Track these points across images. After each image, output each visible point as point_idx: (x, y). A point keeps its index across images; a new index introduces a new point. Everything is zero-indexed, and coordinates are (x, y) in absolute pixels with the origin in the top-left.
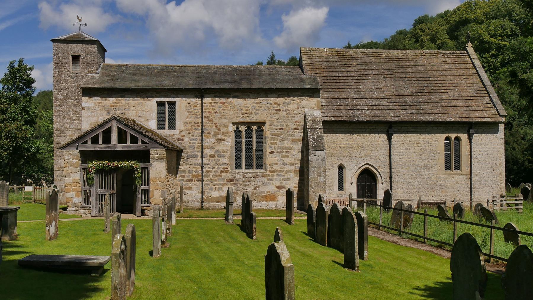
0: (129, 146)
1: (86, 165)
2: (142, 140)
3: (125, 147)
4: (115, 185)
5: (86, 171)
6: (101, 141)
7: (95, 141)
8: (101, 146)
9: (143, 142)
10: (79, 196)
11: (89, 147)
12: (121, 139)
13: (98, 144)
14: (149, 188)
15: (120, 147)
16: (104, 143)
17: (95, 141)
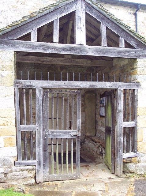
0: (104, 50)
1: (28, 82)
2: (126, 42)
3: (97, 51)
4: (79, 122)
5: (24, 96)
6: (56, 37)
7: (45, 35)
8: (56, 46)
9: (128, 45)
10: (12, 144)
11: (35, 46)
12: (93, 38)
13: (52, 42)
14: (136, 125)
15: (91, 51)
16: (61, 41)
17: (45, 35)
